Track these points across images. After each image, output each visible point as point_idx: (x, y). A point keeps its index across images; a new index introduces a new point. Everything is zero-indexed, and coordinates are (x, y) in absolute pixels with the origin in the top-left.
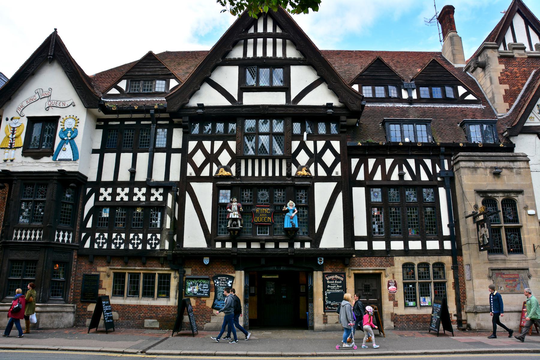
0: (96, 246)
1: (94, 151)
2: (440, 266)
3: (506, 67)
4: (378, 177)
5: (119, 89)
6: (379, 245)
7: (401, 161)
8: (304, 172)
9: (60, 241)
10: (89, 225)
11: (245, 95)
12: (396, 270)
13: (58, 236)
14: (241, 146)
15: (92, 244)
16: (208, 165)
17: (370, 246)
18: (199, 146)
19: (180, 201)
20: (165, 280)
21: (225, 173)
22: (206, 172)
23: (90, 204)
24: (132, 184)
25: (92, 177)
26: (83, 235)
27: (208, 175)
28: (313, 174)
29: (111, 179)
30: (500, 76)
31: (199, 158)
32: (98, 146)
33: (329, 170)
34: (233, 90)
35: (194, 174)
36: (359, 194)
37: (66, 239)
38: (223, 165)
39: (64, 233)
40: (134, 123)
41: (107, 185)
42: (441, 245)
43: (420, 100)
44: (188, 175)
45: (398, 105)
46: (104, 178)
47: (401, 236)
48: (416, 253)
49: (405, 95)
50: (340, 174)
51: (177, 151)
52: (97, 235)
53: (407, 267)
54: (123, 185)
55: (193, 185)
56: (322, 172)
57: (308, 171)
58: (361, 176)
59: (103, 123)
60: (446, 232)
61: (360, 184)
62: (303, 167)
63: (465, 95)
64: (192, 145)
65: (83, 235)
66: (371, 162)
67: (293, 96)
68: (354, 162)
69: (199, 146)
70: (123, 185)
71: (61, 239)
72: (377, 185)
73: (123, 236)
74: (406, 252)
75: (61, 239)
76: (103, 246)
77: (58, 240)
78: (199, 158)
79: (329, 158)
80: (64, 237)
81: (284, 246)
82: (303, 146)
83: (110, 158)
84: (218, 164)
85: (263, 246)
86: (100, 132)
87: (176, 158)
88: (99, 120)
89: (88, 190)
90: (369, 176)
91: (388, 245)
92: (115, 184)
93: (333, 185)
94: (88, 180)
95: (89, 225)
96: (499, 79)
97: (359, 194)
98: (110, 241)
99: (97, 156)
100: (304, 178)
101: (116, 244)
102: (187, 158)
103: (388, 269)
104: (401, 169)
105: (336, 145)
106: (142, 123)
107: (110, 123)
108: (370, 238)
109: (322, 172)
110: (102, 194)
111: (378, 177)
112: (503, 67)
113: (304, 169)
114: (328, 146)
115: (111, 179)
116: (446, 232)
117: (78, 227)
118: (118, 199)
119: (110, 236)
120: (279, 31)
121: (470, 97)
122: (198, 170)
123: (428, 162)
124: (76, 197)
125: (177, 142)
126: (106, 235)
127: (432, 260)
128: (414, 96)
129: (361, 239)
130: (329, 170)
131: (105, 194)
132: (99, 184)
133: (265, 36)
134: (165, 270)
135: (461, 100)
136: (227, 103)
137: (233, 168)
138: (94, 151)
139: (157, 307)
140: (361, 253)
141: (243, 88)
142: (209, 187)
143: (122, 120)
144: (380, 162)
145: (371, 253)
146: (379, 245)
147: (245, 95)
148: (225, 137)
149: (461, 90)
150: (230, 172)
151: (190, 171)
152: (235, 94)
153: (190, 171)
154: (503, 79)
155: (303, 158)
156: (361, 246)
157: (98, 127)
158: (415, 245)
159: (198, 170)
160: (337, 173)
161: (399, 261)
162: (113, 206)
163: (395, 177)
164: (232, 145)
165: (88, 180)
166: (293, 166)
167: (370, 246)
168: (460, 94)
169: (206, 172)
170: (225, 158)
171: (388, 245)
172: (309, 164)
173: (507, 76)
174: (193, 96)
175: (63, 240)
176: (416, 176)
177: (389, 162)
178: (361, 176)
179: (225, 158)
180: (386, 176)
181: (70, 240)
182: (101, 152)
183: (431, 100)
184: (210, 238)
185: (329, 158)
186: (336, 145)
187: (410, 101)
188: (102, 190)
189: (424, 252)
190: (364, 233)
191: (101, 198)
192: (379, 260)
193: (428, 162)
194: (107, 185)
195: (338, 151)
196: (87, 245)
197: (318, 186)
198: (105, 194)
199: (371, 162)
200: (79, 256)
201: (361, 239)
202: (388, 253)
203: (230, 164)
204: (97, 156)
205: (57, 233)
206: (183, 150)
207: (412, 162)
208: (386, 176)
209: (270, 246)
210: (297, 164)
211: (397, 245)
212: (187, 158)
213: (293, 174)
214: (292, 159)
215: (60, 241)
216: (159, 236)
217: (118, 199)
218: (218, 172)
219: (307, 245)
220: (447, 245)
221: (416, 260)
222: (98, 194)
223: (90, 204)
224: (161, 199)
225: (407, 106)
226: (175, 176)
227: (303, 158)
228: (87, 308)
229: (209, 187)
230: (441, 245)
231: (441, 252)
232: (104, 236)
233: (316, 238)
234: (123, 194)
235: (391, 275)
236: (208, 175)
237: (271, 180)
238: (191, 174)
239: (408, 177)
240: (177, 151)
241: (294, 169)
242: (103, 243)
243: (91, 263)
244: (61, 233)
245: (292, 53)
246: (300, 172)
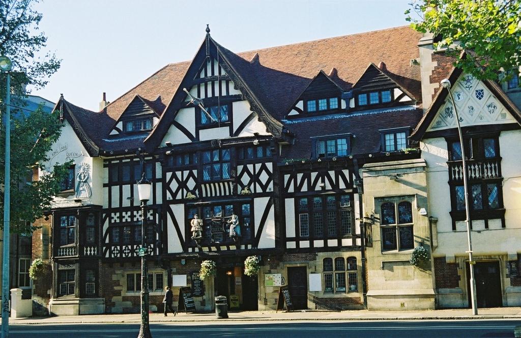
0: (113, 256)
1: (105, 185)
2: (352, 260)
3: (439, 65)
4: (305, 188)
5: (118, 130)
6: (305, 244)
7: (323, 175)
8: (246, 191)
9: (89, 254)
10: (107, 241)
11: (201, 132)
12: (317, 263)
13: (87, 251)
14: (200, 174)
15: (110, 255)
16: (181, 190)
17: (298, 245)
18: (174, 176)
19: (163, 219)
20: (160, 277)
21: (194, 196)
22: (179, 197)
23: (106, 225)
24: (132, 208)
25: (106, 206)
26: (104, 248)
27: (181, 198)
28: (253, 192)
29: (118, 206)
30: (431, 75)
31: (174, 186)
32: (107, 181)
33: (264, 187)
34: (192, 128)
35: (171, 199)
36: (290, 204)
37: (92, 252)
38: (190, 189)
39: (91, 248)
40: (129, 160)
41: (115, 210)
42: (354, 242)
43: (358, 108)
44: (168, 199)
45: (337, 117)
46: (116, 204)
47: (321, 236)
48: (333, 249)
49: (344, 106)
50: (272, 190)
51: (159, 180)
52: (113, 248)
53: (327, 261)
54: (126, 209)
55: (172, 206)
56: (259, 190)
57: (249, 189)
58: (291, 189)
59: (108, 163)
60: (358, 232)
61: (290, 196)
62: (246, 186)
63: (401, 97)
64: (169, 175)
65: (104, 248)
66: (300, 176)
67: (235, 130)
68: (287, 177)
69: (174, 176)
70: (126, 209)
71: (89, 253)
72: (304, 195)
73: (130, 247)
74: (326, 249)
75: (89, 253)
76: (117, 255)
77: (87, 254)
78: (174, 186)
79: (264, 177)
80: (91, 251)
81: (233, 248)
82: (245, 170)
83: (115, 189)
84: (188, 190)
85: (218, 249)
86: (107, 169)
87: (159, 186)
88: (105, 160)
89: (104, 215)
90: (298, 188)
91: (312, 244)
92: (121, 209)
93: (266, 200)
94: (103, 208)
95: (107, 241)
96: (430, 78)
97: (290, 204)
98: (121, 252)
99: (107, 189)
100: (246, 195)
101: (125, 253)
102: (166, 187)
103: (311, 262)
104: (323, 181)
105: (269, 166)
106: (134, 160)
107: (113, 162)
108: (297, 239)
109: (259, 190)
110: (113, 218)
111: (305, 188)
112: (435, 64)
113: (246, 188)
114: (264, 167)
115: (118, 206)
116: (358, 232)
117: (100, 243)
118: (124, 220)
119: (121, 248)
120: (223, 73)
121: (406, 99)
122: (174, 195)
123: (346, 172)
124: (96, 222)
125: (159, 175)
126: (118, 247)
127: (346, 255)
128: (352, 105)
129: (291, 239)
130: (264, 187)
131: (115, 217)
132: (110, 210)
133: (213, 80)
134: (159, 271)
135: (396, 103)
136: (189, 141)
137: (197, 192)
138: (105, 185)
139: (155, 296)
140: (291, 251)
141: (199, 126)
142: (182, 206)
143: (121, 159)
144: (307, 176)
145: (298, 250)
146: (305, 244)
147: (201, 132)
148: (190, 169)
149: (397, 92)
150: (195, 195)
151: (169, 196)
152: (193, 132)
153: (169, 196)
154: (435, 78)
155: (246, 179)
156: (291, 245)
157: (105, 166)
158: (333, 243)
159: (174, 195)
160: (270, 189)
161: (321, 256)
162: (121, 225)
163: (318, 188)
164: (195, 172)
165: (103, 208)
166: (239, 187)
167: (298, 245)
168: (396, 97)
169: (179, 197)
170: (191, 184)
171: (312, 244)
172: (250, 184)
173: (439, 73)
174: (165, 137)
175: (91, 254)
176: (335, 186)
177: (314, 175)
178: (291, 189)
179: (191, 184)
180: (311, 187)
181: (96, 253)
182: (109, 185)
183: (369, 107)
184: (185, 245)
185: (264, 177)
186: (269, 166)
187: (349, 110)
188: (113, 215)
189: (340, 248)
190: (294, 235)
191: (113, 221)
192: (304, 255)
193: (346, 172)
194: (115, 210)
195: (271, 170)
196: (107, 256)
197: (257, 201)
198: (115, 217)
199: (300, 176)
200: (103, 263)
201: (291, 239)
202: (312, 250)
203: (195, 189)
204: (107, 189)
205: (85, 249)
206: (163, 180)
207: (332, 174)
208: (311, 187)
209: (224, 248)
210: (242, 184)
211: (319, 244)
212: (166, 187)
213: (239, 193)
214: (238, 180)
215: (89, 254)
216: (152, 246)
217: (124, 220)
218: (186, 196)
219: (250, 247)
220: (359, 242)
221: (333, 256)
222: (111, 218)
223: (106, 225)
224: (151, 218)
225: (345, 116)
226: (159, 201)
227: (246, 179)
228: (111, 300)
229: (182, 206)
230: (354, 242)
231: (353, 248)
232: (117, 248)
233: (256, 241)
234: (127, 216)
235: (314, 267)
236: (181, 198)
237: (224, 199)
238: (169, 198)
239: (329, 187)
240: (159, 180)
241: (239, 188)
242: (117, 254)
243: (111, 266)
244: (89, 249)
245: (233, 92)
246: (243, 191)
